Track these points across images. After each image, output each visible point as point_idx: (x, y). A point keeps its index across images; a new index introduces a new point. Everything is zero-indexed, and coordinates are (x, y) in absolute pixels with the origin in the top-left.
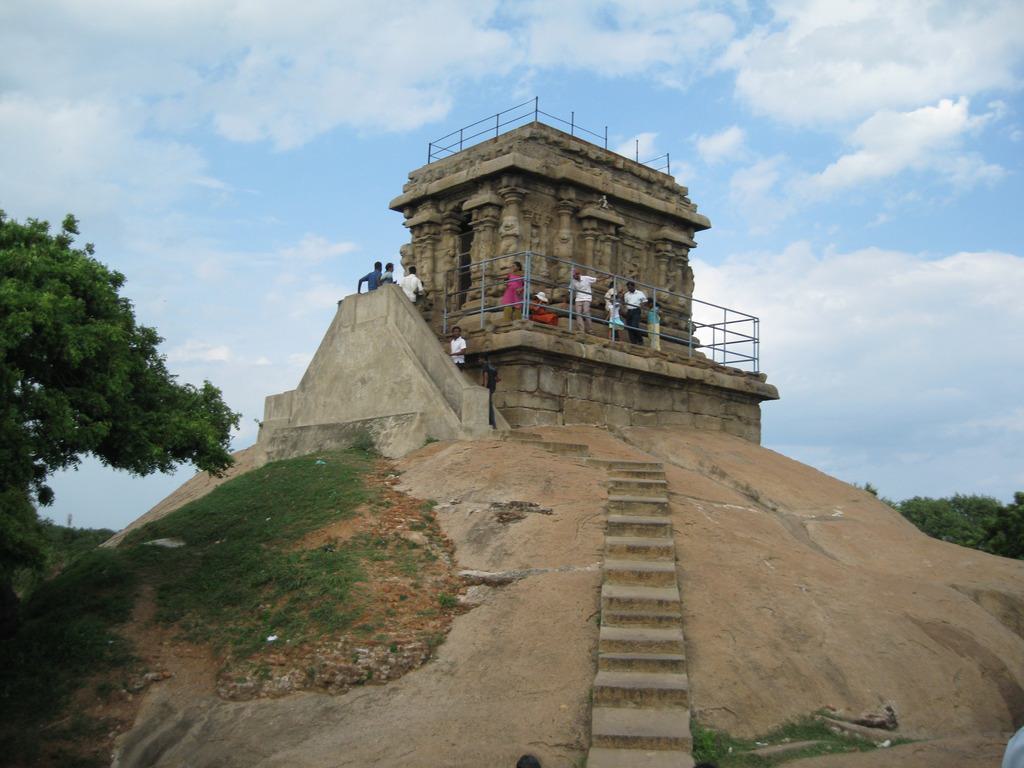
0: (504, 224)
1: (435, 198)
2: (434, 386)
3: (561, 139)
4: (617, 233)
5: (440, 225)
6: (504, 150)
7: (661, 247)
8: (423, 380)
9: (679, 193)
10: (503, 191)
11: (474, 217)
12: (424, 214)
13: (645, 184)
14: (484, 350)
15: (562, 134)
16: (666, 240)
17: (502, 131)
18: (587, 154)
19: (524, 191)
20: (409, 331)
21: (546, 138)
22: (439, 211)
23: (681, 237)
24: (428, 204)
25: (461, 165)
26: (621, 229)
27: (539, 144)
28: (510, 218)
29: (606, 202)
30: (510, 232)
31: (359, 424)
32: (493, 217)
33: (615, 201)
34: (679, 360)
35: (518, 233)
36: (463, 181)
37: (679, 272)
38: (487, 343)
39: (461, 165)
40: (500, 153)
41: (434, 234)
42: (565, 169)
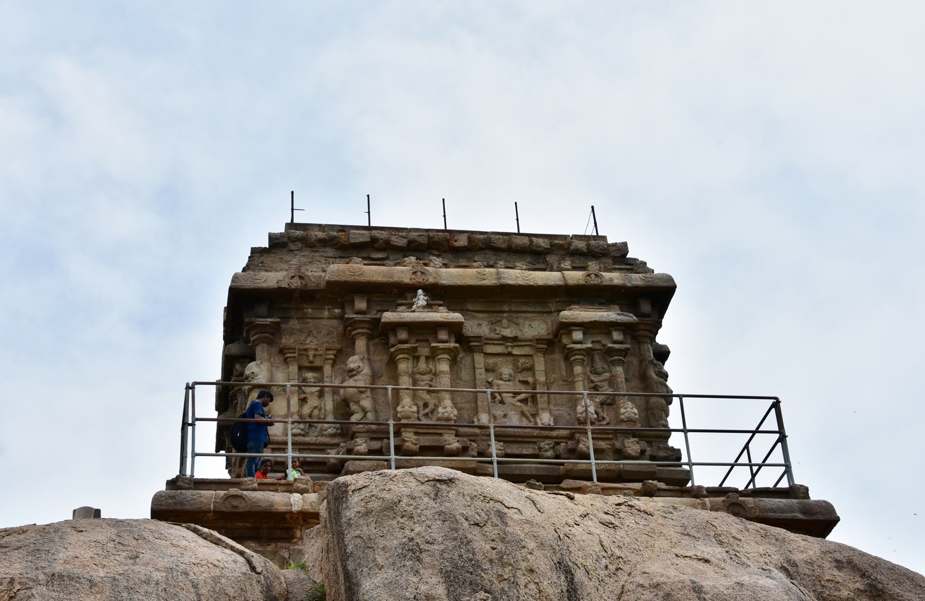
9: (617, 255)
27: (291, 251)
33: (440, 294)
42: (340, 270)
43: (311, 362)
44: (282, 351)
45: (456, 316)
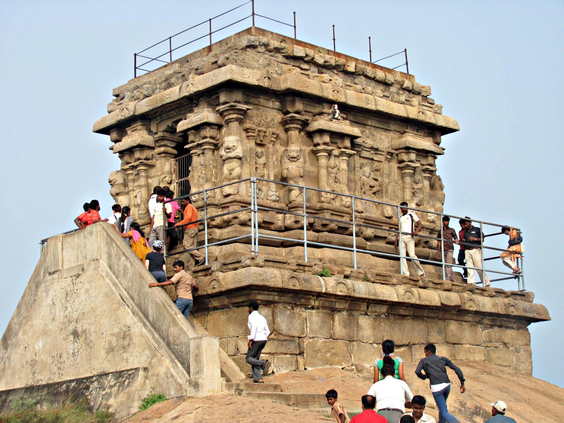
0: (225, 145)
1: (145, 119)
2: (157, 336)
3: (283, 45)
4: (354, 146)
5: (153, 148)
6: (220, 62)
7: (404, 157)
8: (144, 330)
10: (221, 108)
11: (191, 138)
12: (136, 136)
13: (382, 87)
14: (210, 292)
15: (284, 39)
16: (408, 149)
17: (216, 38)
18: (313, 59)
19: (245, 107)
20: (125, 274)
21: (266, 45)
22: (150, 132)
23: (426, 143)
24: (138, 125)
25: (173, 80)
26: (358, 141)
28: (233, 140)
29: (338, 111)
30: (232, 155)
31: (73, 384)
32: (212, 137)
34: (431, 285)
35: (241, 155)
36: (176, 98)
37: (426, 183)
38: (213, 283)
39: (173, 80)
40: (216, 65)
41: (147, 159)
42: (292, 78)
43: (261, 141)
44: (246, 130)
45: (355, 131)
